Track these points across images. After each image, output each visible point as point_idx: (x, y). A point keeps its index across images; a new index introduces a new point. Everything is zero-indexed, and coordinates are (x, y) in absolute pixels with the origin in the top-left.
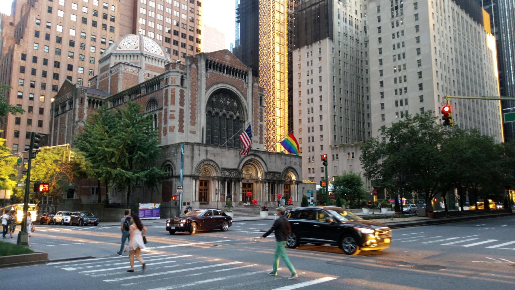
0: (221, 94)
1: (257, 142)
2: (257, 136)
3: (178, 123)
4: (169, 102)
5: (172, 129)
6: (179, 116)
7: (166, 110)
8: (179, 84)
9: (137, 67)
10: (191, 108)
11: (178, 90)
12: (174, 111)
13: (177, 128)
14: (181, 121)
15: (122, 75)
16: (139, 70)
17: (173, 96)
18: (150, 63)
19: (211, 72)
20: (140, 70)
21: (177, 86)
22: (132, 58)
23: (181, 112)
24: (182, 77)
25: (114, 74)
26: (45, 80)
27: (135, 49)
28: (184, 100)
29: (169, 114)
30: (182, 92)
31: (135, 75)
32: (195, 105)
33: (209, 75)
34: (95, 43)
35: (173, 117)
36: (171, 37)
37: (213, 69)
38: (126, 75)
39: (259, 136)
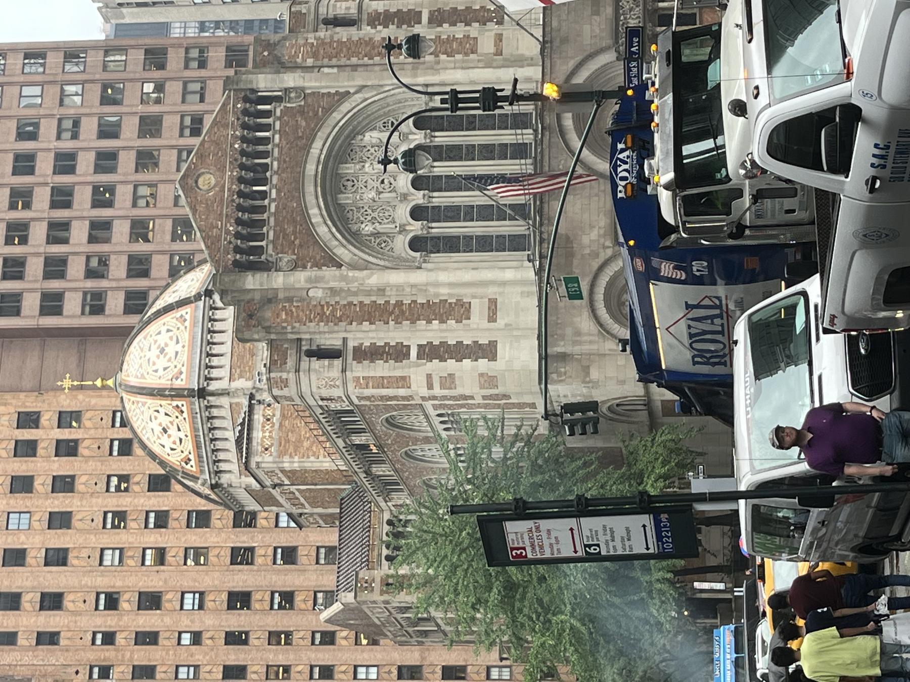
0: (346, 199)
1: (499, 38)
2: (476, 39)
3: (467, 362)
4: (402, 392)
5: (489, 380)
6: (442, 359)
7: (423, 398)
8: (337, 363)
9: (251, 407)
10: (413, 322)
11: (359, 370)
12: (429, 377)
13: (483, 364)
14: (459, 352)
15: (286, 458)
16: (259, 402)
17: (381, 382)
18: (225, 361)
19: (275, 248)
20: (258, 397)
21: (344, 371)
22: (217, 423)
23: (430, 352)
24: (310, 354)
25: (284, 479)
26: (301, 634)
27: (185, 415)
28: (387, 344)
29: (437, 391)
30: (361, 354)
31: (278, 413)
32: (399, 304)
33: (286, 258)
34: (136, 479)
35: (449, 381)
36: (46, 184)
37: (261, 237)
38: (285, 446)
39: (474, 30)
